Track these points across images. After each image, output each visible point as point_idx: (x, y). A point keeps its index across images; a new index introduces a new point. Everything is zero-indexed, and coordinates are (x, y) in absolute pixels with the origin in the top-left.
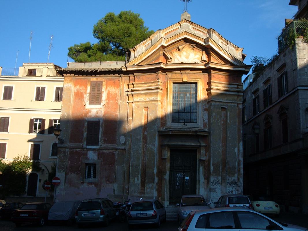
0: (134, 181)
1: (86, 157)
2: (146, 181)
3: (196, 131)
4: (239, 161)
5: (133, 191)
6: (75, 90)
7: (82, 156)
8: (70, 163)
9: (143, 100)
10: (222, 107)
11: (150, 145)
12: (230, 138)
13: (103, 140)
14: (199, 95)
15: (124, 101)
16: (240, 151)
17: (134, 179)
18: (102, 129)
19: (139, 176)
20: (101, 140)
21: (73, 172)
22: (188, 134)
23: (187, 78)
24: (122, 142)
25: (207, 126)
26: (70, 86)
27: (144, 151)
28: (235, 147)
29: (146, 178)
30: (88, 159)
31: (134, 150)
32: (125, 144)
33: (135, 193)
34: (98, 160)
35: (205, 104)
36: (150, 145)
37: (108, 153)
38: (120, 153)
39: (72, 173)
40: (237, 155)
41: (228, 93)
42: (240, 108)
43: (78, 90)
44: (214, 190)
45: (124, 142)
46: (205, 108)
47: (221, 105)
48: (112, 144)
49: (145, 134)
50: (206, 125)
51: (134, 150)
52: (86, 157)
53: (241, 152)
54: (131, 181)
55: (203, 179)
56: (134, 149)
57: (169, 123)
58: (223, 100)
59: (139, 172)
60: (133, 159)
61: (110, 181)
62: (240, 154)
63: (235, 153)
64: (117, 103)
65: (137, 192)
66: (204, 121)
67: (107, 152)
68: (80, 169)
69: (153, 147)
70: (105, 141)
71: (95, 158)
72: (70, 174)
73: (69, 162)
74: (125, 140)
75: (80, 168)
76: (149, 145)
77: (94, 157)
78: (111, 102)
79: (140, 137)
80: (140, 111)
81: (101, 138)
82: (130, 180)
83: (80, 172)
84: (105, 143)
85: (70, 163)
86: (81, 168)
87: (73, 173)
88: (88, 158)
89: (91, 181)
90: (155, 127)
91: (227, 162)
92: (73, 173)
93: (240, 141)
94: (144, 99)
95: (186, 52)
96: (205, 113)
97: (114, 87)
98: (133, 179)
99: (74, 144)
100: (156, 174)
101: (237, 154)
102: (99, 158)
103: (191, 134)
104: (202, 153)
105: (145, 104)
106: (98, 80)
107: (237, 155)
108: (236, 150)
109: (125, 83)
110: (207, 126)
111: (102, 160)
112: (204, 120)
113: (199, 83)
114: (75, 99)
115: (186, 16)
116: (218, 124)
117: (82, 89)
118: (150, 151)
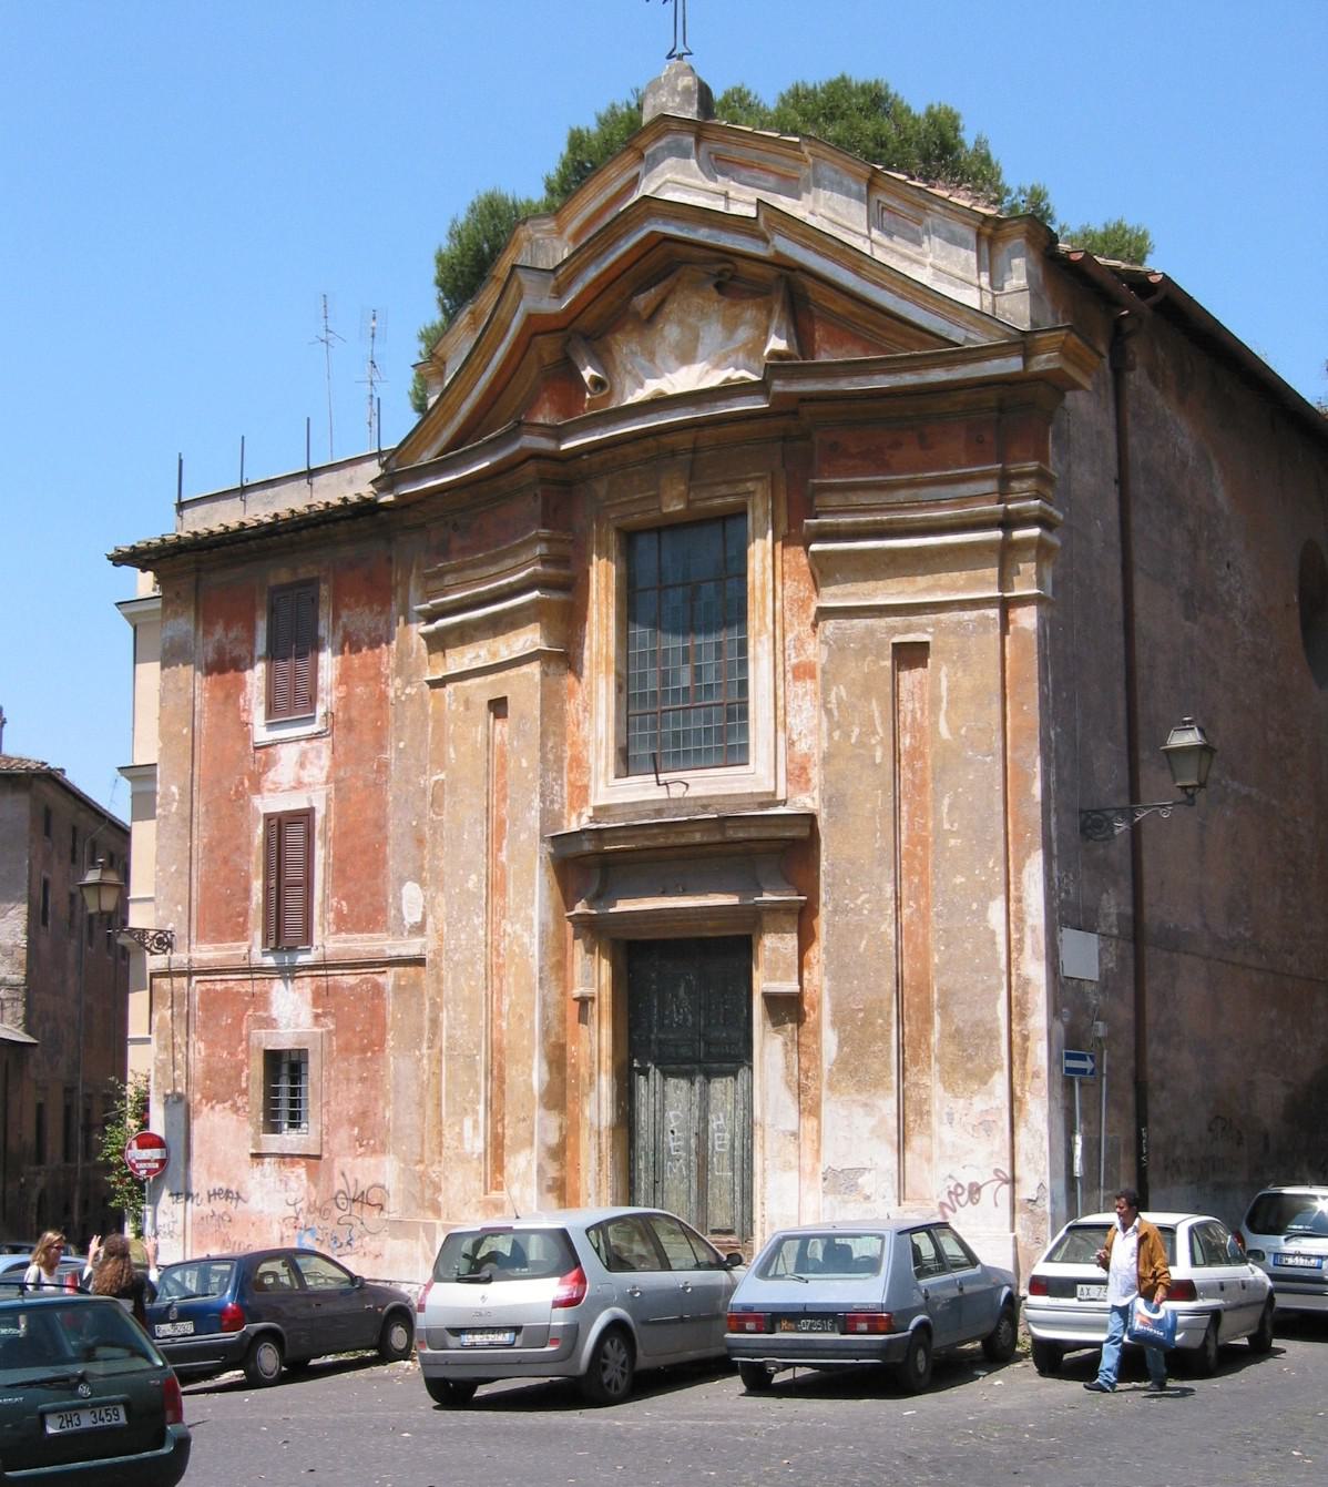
1: (265, 1015)
3: (722, 821)
7: (250, 1012)
8: (203, 1054)
10: (897, 639)
11: (518, 926)
12: (952, 842)
13: (331, 916)
14: (758, 584)
15: (414, 679)
20: (323, 913)
21: (217, 1102)
22: (683, 840)
23: (682, 488)
25: (815, 775)
26: (185, 629)
28: (992, 897)
30: (269, 1023)
32: (419, 929)
35: (798, 638)
37: (352, 988)
39: (212, 1108)
42: (1025, 630)
45: (418, 918)
46: (794, 661)
47: (893, 630)
49: (502, 862)
50: (804, 769)
53: (1034, 930)
55: (793, 1112)
58: (899, 593)
60: (451, 1013)
62: (1028, 941)
63: (993, 932)
64: (383, 697)
66: (791, 744)
67: (349, 980)
68: (244, 1085)
71: (303, 1014)
72: (205, 1109)
73: (201, 1045)
75: (244, 1079)
77: (298, 1015)
80: (477, 726)
84: (339, 930)
85: (203, 1054)
86: (248, 1078)
88: (274, 1020)
90: (533, 813)
93: (1028, 855)
95: (681, 322)
96: (796, 696)
99: (216, 949)
102: (317, 1016)
103: (698, 837)
104: (774, 950)
106: (302, 577)
109: (414, 571)
112: (795, 737)
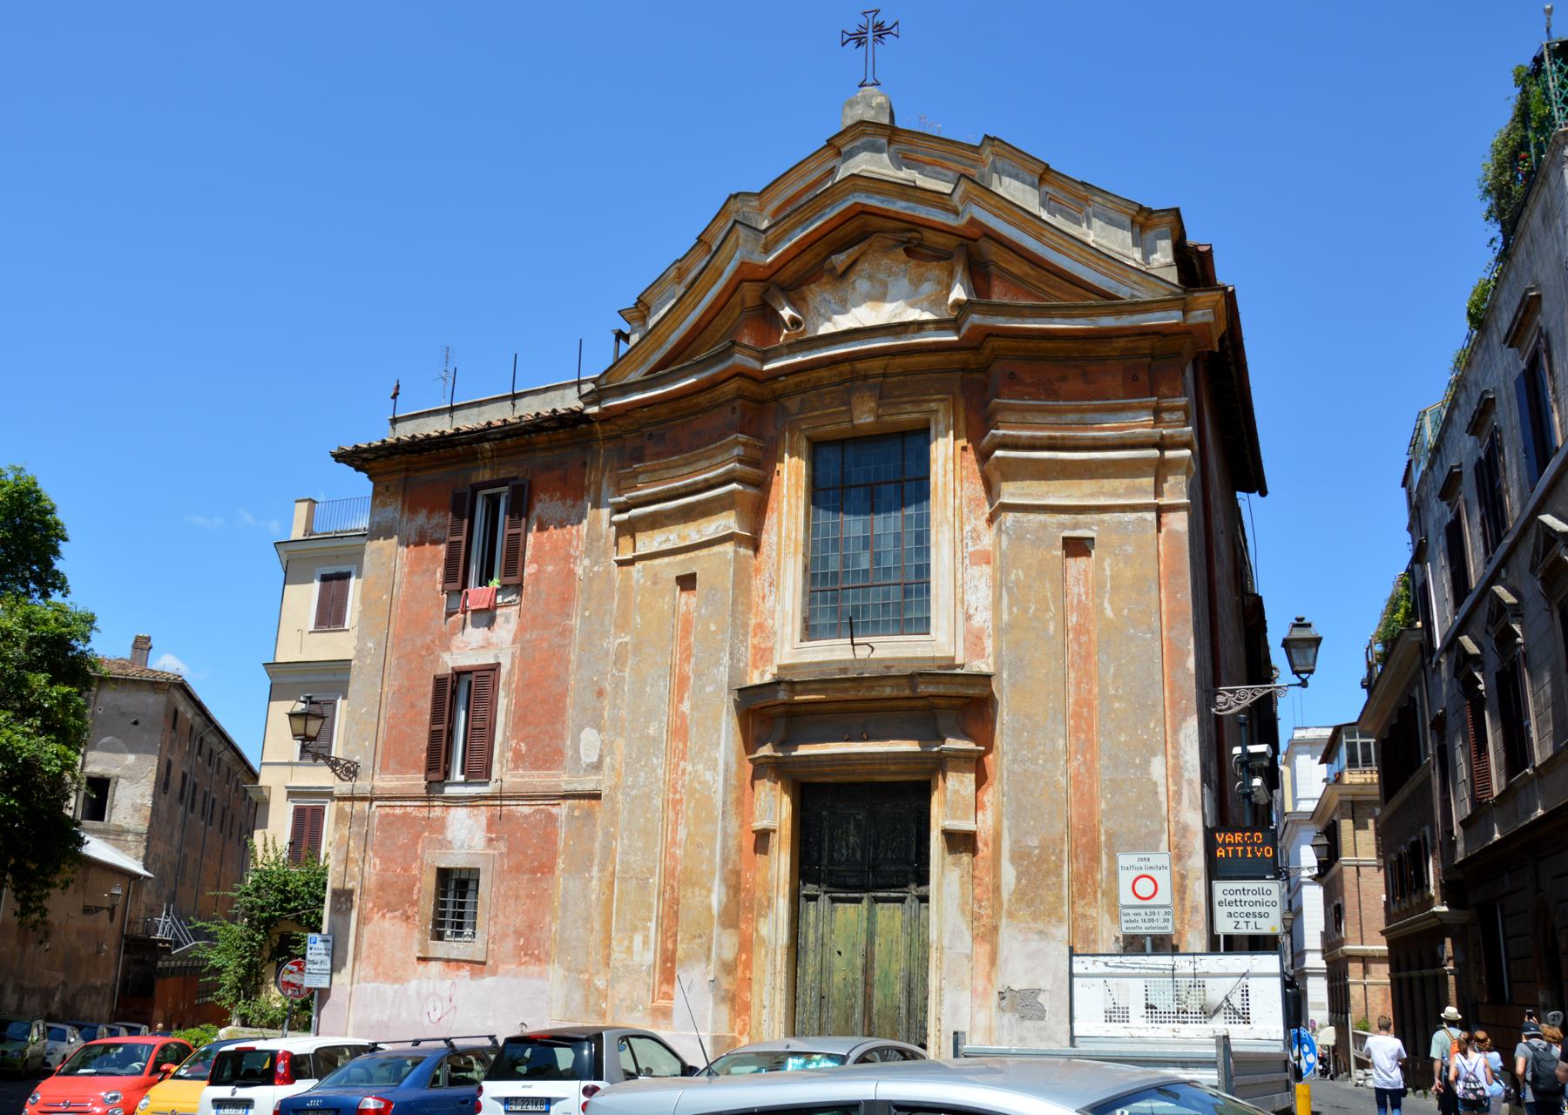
0: (629, 949)
1: (440, 837)
2: (681, 949)
3: (913, 678)
4: (1184, 830)
5: (623, 1000)
6: (410, 535)
7: (426, 834)
8: (378, 868)
9: (677, 541)
10: (1068, 533)
11: (700, 767)
12: (1117, 705)
13: (510, 755)
14: (940, 484)
15: (602, 560)
16: (1186, 775)
17: (631, 942)
18: (506, 701)
19: (652, 925)
20: (502, 753)
21: (389, 911)
22: (874, 694)
23: (873, 404)
24: (589, 760)
25: (989, 644)
26: (391, 516)
27: (678, 796)
28: (1153, 753)
29: (679, 938)
30: (445, 844)
31: (634, 793)
32: (597, 767)
33: (633, 1015)
34: (488, 851)
35: (974, 530)
36: (700, 767)
37: (526, 817)
38: (577, 813)
39: (383, 916)
40: (1162, 797)
41: (652, 375)
42: (1176, 531)
43: (420, 532)
44: (62, 1037)
45: (595, 759)
46: (971, 549)
47: (1063, 526)
48: (549, 769)
49: (683, 713)
50: (979, 638)
51: (634, 793)
52: (440, 837)
53: (1190, 783)
54: (617, 955)
55: (968, 938)
56: (633, 787)
57: (787, 648)
58: (1067, 497)
59: (649, 908)
60: (626, 841)
61: (533, 953)
62: (1185, 792)
63: (1155, 784)
64: (571, 573)
65: (641, 1007)
66: (969, 617)
67: (524, 809)
68: (415, 897)
69: (709, 776)
70: (518, 760)
71: (476, 838)
72: (376, 917)
73: (377, 861)
74: (598, 745)
75: (415, 892)
76: (694, 765)
77: (472, 838)
78: (550, 568)
79: (660, 728)
80: (663, 598)
81: (501, 745)
82: (614, 943)
83: (415, 909)
84: (516, 767)
85: (378, 868)
86: (419, 892)
87: (388, 916)
88: (450, 842)
89: (455, 952)
90: (721, 668)
91: (1103, 838)
92: (388, 916)
93: (1184, 719)
94: (679, 536)
95: (871, 278)
96: (973, 577)
97: (564, 498)
98: (626, 943)
99: (398, 779)
100: (719, 914)
101: (1162, 790)
102: (490, 840)
103: (888, 692)
104: (956, 792)
105: (683, 562)
106: (501, 476)
107: (1162, 797)
108: (1158, 768)
109: (607, 472)
110: (989, 644)
111: (504, 850)
112: (971, 611)
113: (937, 423)
114: (411, 573)
115: (869, 106)
116: (1046, 629)
117: (437, 525)
118: (697, 796)
